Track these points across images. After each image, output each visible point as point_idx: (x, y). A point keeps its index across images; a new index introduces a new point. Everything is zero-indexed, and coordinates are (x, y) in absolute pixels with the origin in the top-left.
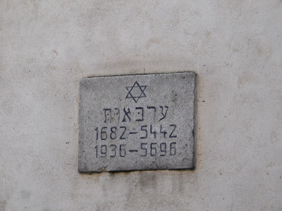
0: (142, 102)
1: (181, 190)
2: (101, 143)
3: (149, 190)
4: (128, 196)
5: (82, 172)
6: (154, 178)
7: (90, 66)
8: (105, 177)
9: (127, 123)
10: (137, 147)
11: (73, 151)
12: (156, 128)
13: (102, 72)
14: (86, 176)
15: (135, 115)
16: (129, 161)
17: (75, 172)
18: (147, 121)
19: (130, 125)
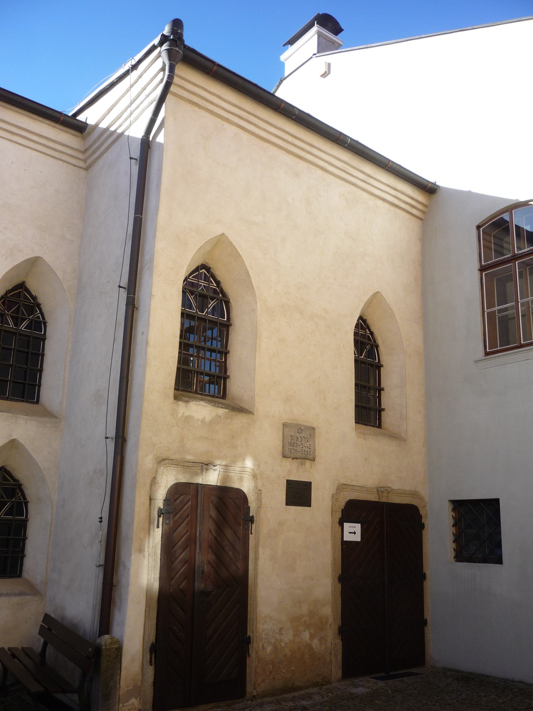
0: (302, 435)
1: (311, 467)
2: (290, 447)
3: (303, 466)
4: (297, 467)
5: (283, 457)
6: (304, 462)
7: (285, 418)
8: (290, 460)
9: (297, 442)
10: (300, 451)
11: (280, 448)
12: (306, 445)
13: (289, 422)
14: (285, 459)
15: (300, 439)
16: (298, 455)
17: (281, 456)
18: (303, 442)
19: (299, 443)
